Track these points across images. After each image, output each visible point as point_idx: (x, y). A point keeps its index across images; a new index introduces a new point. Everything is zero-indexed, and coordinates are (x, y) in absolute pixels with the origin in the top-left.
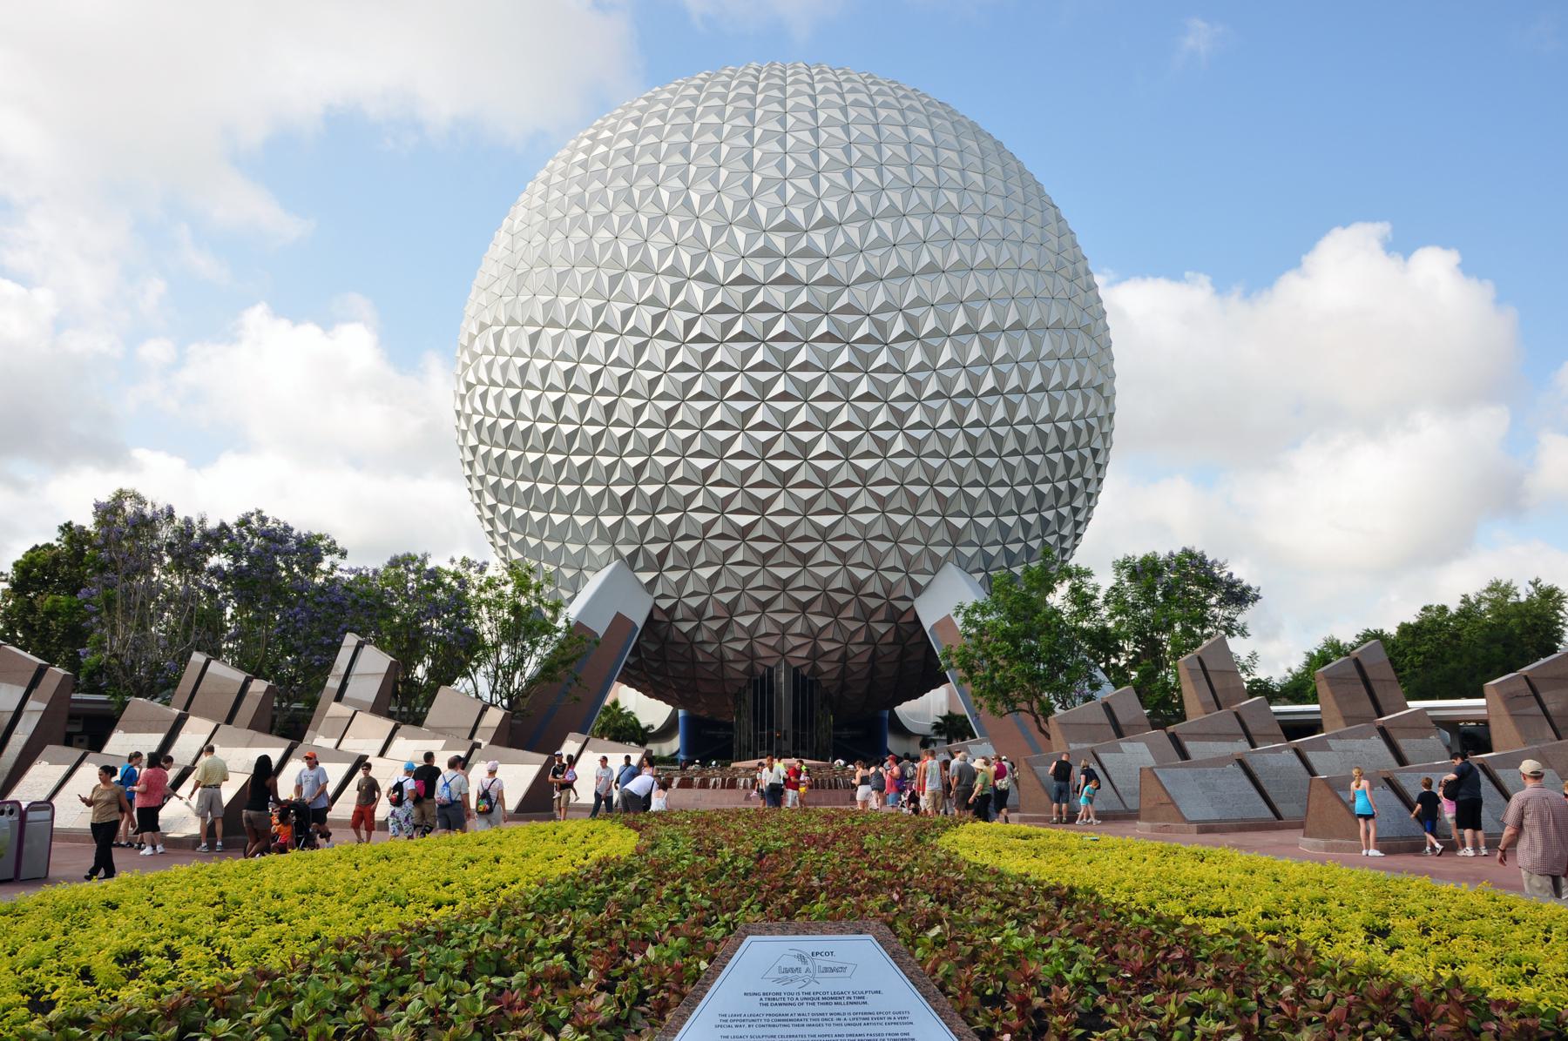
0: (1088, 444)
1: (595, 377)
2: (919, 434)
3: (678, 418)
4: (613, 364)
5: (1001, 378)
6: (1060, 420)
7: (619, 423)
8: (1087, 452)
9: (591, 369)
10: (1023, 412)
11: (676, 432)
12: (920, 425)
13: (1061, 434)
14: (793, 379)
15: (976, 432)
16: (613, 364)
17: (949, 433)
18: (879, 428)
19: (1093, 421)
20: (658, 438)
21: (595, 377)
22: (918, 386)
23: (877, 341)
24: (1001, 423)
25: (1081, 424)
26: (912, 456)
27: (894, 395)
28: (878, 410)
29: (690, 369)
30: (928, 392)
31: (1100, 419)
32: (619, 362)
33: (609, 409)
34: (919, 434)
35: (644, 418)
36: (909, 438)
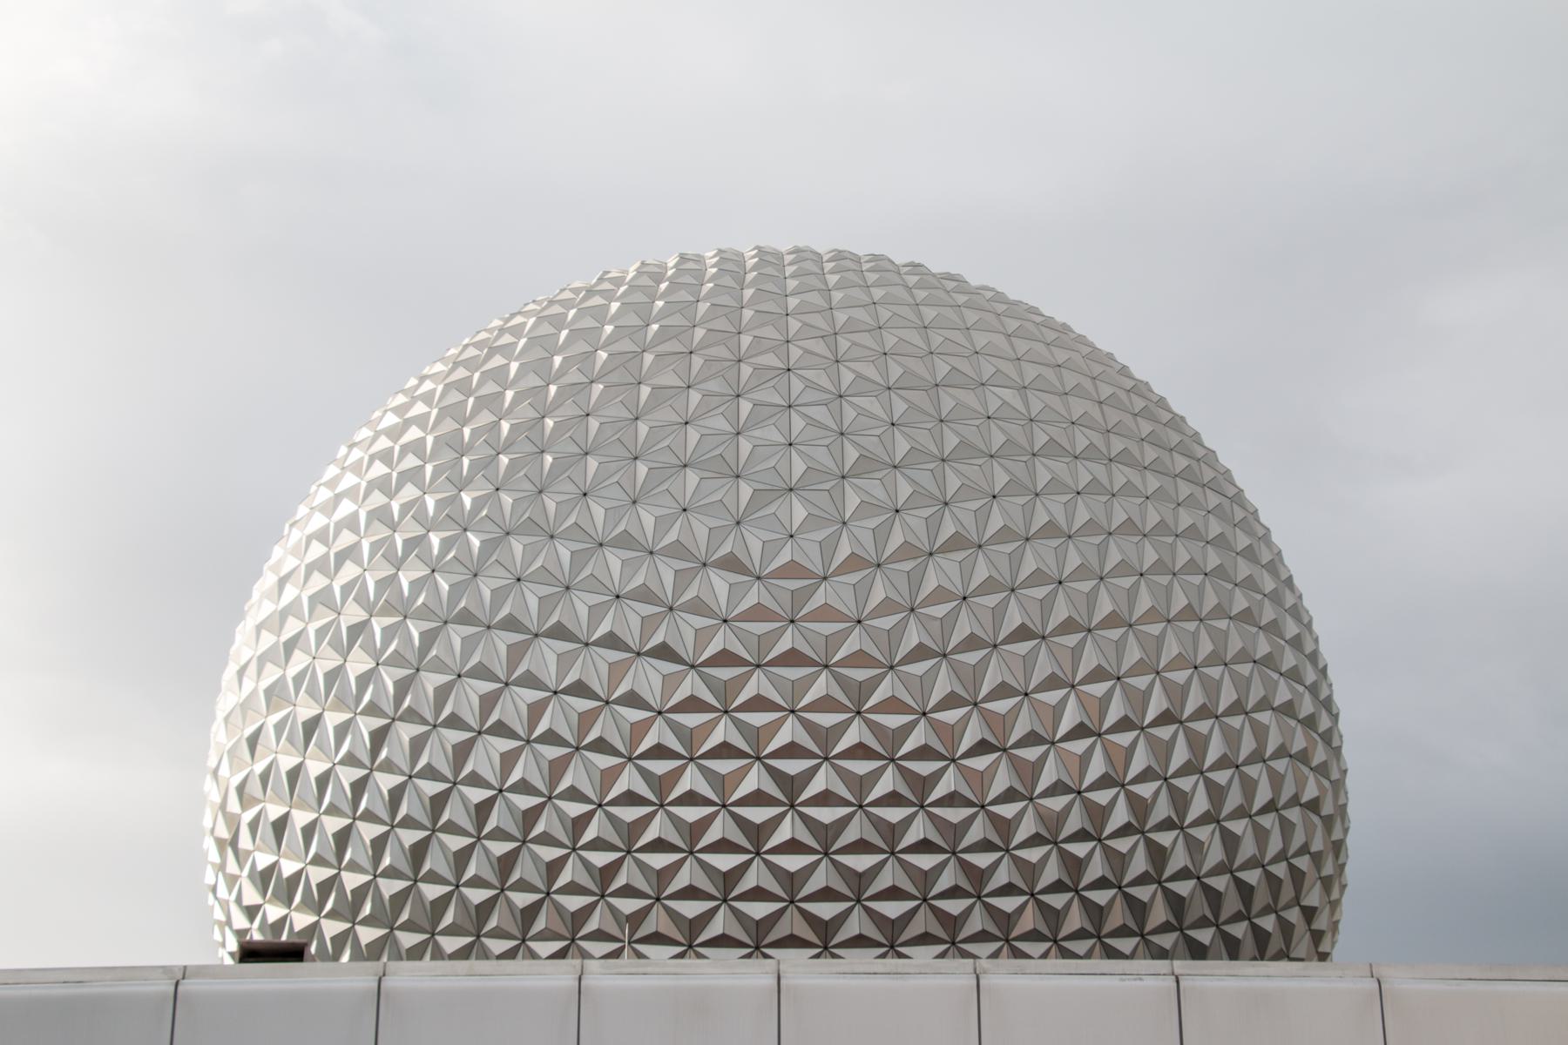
0: (1297, 900)
1: (484, 809)
2: (1008, 904)
3: (620, 881)
4: (513, 789)
5: (1140, 807)
6: (1244, 867)
7: (523, 886)
8: (1294, 915)
9: (477, 795)
10: (1179, 860)
11: (618, 903)
12: (1008, 890)
13: (1245, 891)
14: (806, 819)
15: (1101, 897)
16: (515, 789)
17: (1057, 901)
18: (944, 895)
19: (1303, 863)
20: (587, 911)
21: (484, 809)
22: (1005, 827)
23: (938, 756)
24: (1142, 880)
25: (1280, 870)
26: (997, 939)
27: (965, 843)
28: (941, 867)
29: (641, 801)
30: (1021, 835)
31: (1317, 859)
32: (524, 787)
33: (506, 864)
34: (1008, 904)
35: (564, 878)
36: (992, 911)
